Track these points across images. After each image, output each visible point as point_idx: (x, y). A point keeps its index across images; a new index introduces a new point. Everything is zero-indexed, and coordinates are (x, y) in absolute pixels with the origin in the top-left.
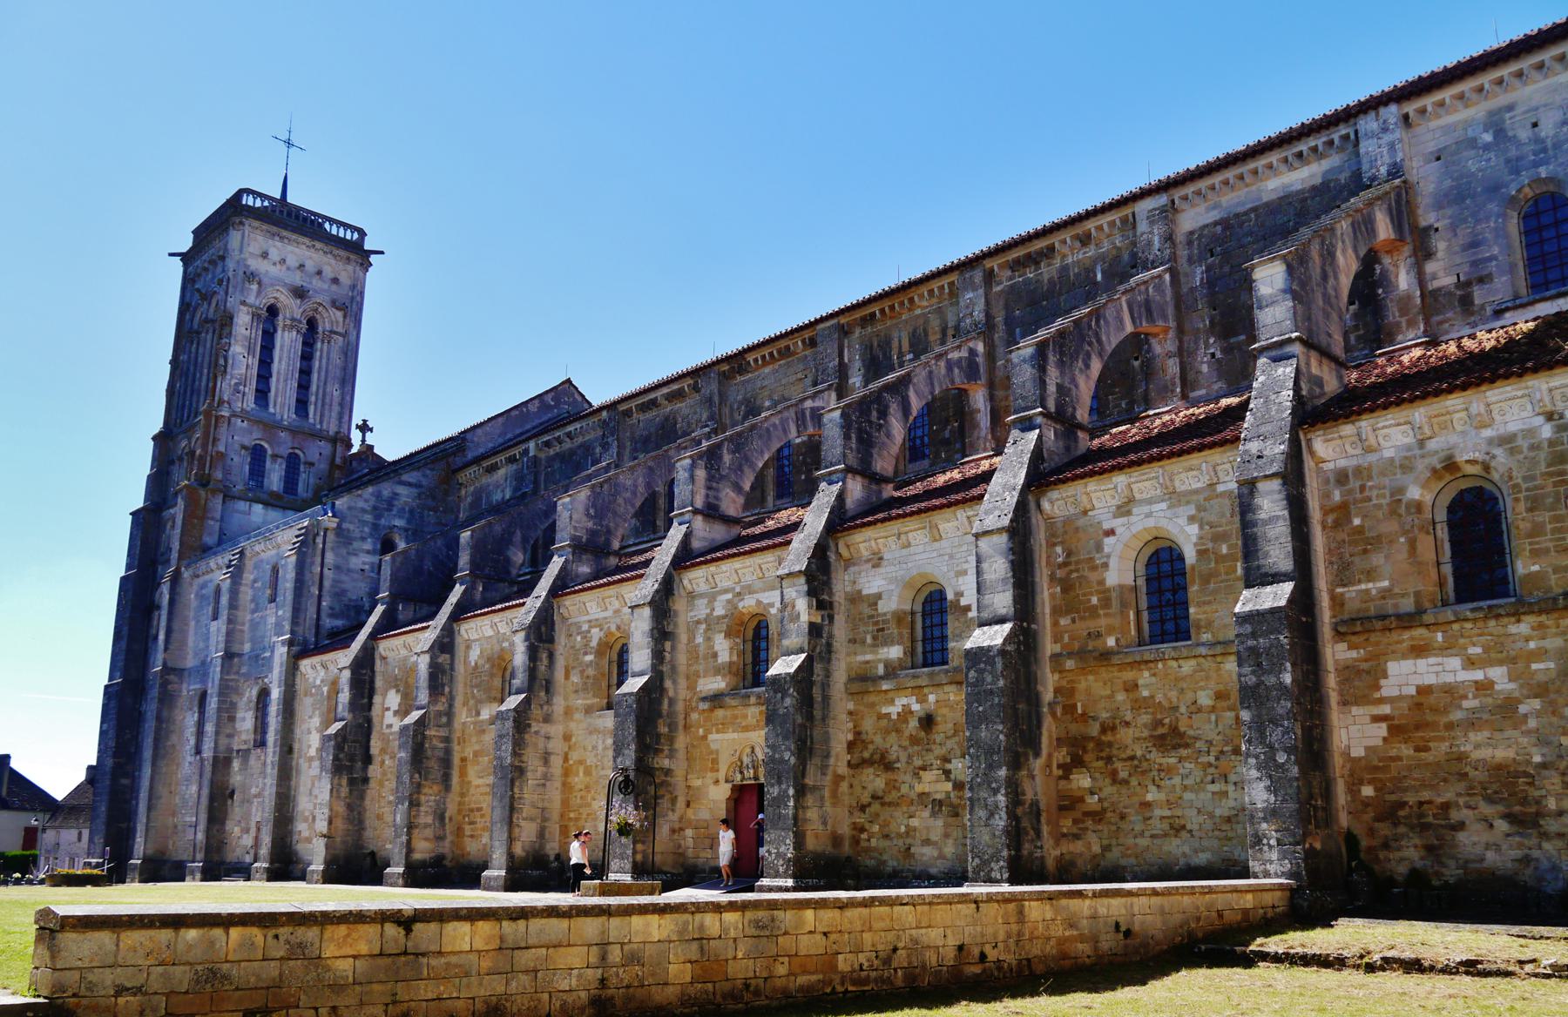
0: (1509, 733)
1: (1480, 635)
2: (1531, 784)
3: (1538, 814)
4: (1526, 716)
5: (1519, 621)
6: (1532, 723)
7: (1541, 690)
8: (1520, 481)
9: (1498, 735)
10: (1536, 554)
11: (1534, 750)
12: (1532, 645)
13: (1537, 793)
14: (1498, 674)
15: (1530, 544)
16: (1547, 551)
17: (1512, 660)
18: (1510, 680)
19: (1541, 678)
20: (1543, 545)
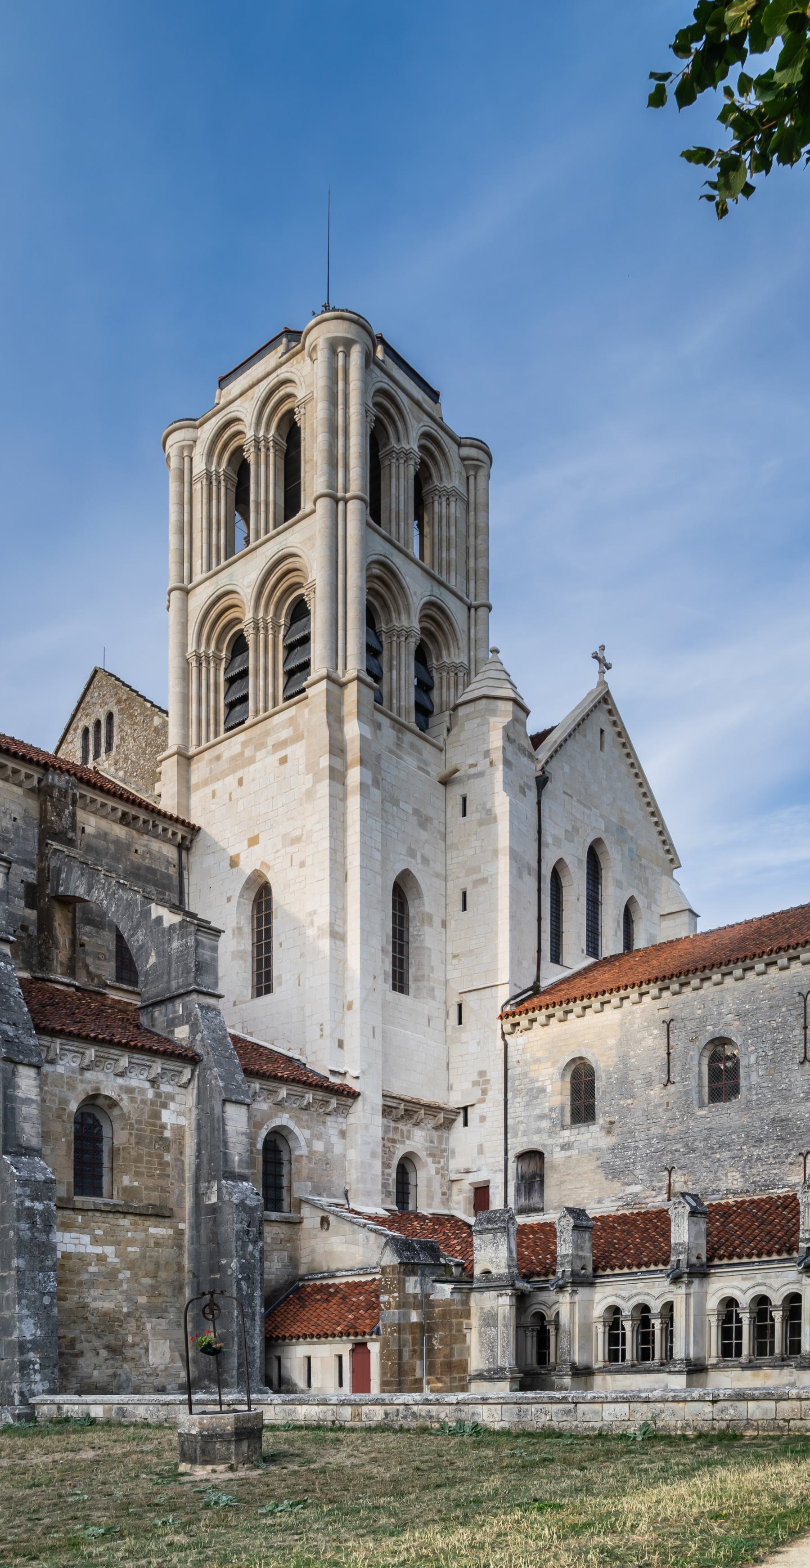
0: (113, 1292)
1: (103, 1222)
2: (120, 1326)
3: (123, 1346)
4: (122, 1281)
5: (125, 1218)
6: (125, 1286)
7: (131, 1266)
8: (134, 1121)
9: (106, 1293)
10: (138, 1174)
11: (124, 1304)
12: (129, 1234)
13: (124, 1332)
14: (109, 1250)
15: (135, 1167)
16: (142, 1174)
17: (118, 1243)
18: (116, 1256)
19: (132, 1257)
20: (141, 1170)
